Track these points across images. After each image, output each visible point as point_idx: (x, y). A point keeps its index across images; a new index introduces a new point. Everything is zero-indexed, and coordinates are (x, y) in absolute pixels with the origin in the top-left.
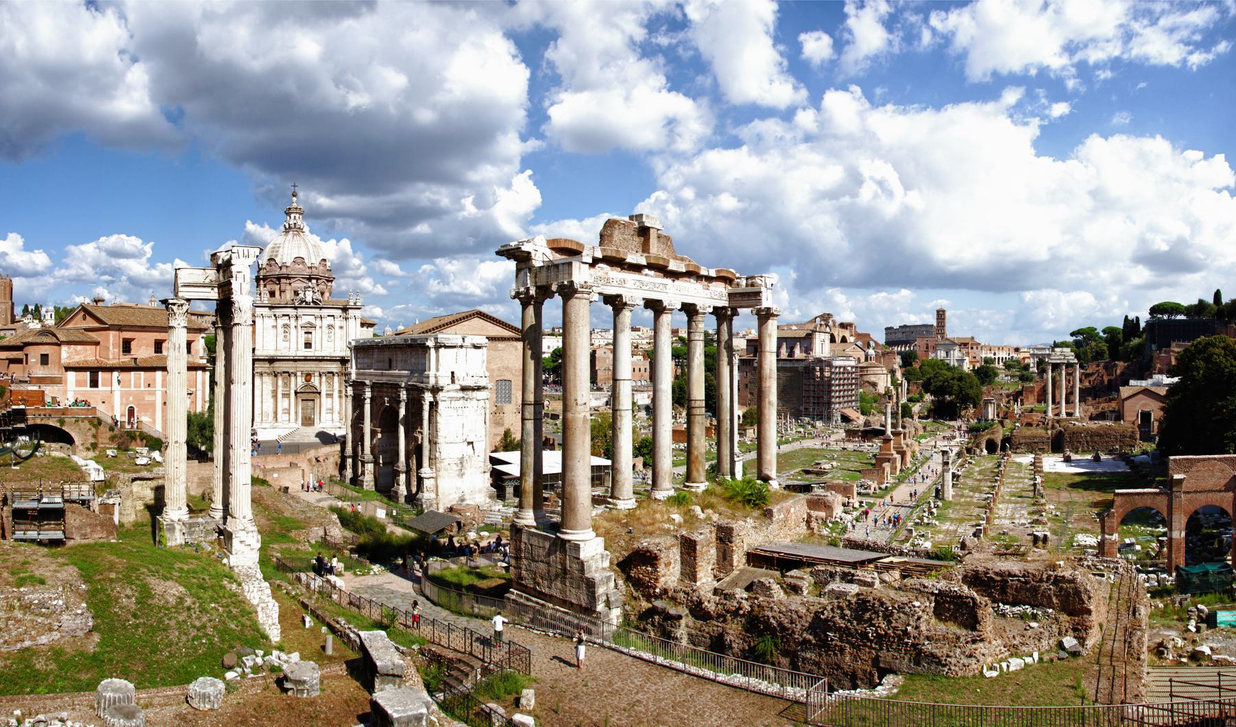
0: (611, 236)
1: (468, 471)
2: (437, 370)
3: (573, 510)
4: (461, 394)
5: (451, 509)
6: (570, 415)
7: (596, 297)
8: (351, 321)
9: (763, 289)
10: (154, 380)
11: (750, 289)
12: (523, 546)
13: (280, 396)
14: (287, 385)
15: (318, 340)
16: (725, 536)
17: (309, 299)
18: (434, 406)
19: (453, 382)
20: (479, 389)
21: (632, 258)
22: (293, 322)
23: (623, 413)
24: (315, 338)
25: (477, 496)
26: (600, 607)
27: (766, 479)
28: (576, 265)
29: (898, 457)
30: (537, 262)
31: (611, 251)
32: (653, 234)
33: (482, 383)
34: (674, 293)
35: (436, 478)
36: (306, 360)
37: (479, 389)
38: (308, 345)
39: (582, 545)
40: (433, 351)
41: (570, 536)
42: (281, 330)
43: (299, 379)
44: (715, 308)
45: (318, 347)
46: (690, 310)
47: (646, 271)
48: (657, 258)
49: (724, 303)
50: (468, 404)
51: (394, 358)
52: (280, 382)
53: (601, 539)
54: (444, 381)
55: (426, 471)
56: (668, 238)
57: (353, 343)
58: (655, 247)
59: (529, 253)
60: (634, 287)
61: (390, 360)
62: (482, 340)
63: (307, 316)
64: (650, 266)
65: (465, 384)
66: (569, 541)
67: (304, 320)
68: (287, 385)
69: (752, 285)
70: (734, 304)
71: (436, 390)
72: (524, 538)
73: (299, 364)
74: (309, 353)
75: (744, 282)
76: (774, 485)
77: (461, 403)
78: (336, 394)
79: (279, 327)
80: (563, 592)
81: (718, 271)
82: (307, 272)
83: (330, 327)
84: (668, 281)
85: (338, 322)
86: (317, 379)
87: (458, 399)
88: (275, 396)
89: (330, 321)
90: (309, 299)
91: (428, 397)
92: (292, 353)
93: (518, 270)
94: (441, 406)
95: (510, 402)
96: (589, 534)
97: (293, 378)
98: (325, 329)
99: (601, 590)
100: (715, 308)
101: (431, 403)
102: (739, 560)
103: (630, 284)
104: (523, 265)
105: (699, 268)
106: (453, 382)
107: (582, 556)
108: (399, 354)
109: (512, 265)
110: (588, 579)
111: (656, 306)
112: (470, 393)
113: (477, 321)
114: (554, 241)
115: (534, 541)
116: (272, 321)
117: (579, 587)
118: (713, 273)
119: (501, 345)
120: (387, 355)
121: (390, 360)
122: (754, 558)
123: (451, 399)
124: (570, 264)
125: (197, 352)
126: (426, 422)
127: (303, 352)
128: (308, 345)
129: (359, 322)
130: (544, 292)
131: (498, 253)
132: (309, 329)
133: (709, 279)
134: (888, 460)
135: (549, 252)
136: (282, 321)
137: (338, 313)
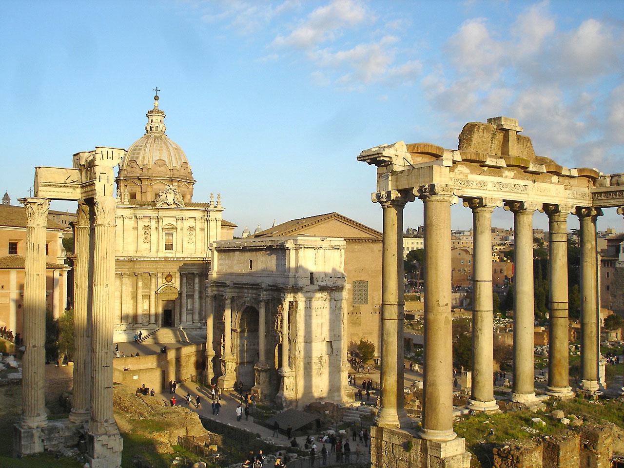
0: (470, 140)
3: (434, 410)
6: (431, 316)
7: (456, 200)
8: (212, 224)
10: (9, 281)
11: (613, 189)
12: (384, 444)
13: (140, 297)
14: (147, 286)
15: (179, 241)
17: (170, 200)
19: (312, 283)
22: (154, 222)
23: (485, 315)
24: (176, 240)
28: (436, 168)
30: (399, 166)
31: (471, 153)
32: (512, 136)
34: (536, 194)
36: (166, 260)
38: (169, 247)
39: (443, 445)
40: (293, 253)
41: (434, 435)
42: (141, 232)
43: (160, 280)
44: (579, 209)
45: (179, 248)
46: (551, 210)
47: (507, 173)
48: (518, 158)
49: (586, 203)
51: (254, 259)
52: (140, 284)
53: (462, 441)
56: (528, 140)
57: (215, 245)
58: (515, 150)
60: (494, 189)
62: (341, 242)
63: (168, 219)
65: (323, 284)
66: (431, 441)
67: (165, 222)
68: (147, 286)
69: (618, 184)
70: (598, 204)
72: (385, 437)
73: (161, 266)
74: (169, 254)
75: (608, 181)
78: (197, 296)
79: (140, 228)
81: (580, 171)
82: (170, 174)
83: (192, 229)
84: (529, 183)
85: (199, 225)
86: (178, 280)
88: (135, 297)
89: (191, 223)
90: (170, 200)
92: (153, 254)
93: (380, 175)
95: (367, 303)
96: (450, 435)
97: (153, 280)
98: (186, 232)
100: (579, 209)
101: (291, 303)
103: (490, 186)
104: (384, 170)
106: (312, 283)
111: (515, 207)
116: (130, 223)
118: (575, 173)
119: (357, 247)
120: (248, 256)
121: (251, 261)
124: (431, 168)
125: (54, 253)
126: (286, 322)
127: (164, 253)
128: (169, 247)
129: (219, 223)
130: (407, 195)
131: (361, 158)
132: (170, 231)
135: (409, 156)
136: (141, 224)
137: (198, 215)
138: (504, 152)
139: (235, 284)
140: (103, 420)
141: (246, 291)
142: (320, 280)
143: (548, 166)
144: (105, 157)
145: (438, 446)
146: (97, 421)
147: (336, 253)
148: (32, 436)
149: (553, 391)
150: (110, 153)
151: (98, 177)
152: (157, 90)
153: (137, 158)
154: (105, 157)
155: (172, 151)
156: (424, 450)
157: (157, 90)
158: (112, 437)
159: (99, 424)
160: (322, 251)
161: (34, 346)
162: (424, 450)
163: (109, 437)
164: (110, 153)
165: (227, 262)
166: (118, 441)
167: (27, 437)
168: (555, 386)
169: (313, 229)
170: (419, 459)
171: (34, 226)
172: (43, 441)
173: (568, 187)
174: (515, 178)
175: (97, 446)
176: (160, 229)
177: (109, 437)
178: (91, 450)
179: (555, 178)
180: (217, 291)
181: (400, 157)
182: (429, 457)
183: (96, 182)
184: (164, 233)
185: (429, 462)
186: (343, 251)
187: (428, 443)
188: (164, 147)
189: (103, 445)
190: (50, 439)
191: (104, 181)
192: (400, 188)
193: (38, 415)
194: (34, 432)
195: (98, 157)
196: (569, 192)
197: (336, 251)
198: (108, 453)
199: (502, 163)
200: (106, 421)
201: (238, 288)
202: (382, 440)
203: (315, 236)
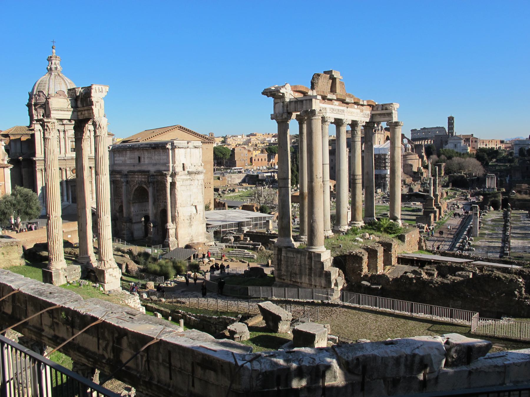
1: (195, 223)
2: (174, 162)
4: (188, 177)
5: (188, 247)
9: (393, 111)
16: (387, 247)
18: (173, 184)
20: (198, 173)
21: (329, 96)
22: (62, 134)
25: (200, 237)
26: (333, 286)
27: (395, 219)
29: (437, 210)
32: (338, 81)
33: (201, 169)
35: (176, 229)
37: (198, 173)
43: (68, 172)
50: (192, 183)
51: (142, 156)
54: (179, 169)
55: (170, 225)
59: (283, 94)
61: (139, 158)
64: (338, 100)
65: (190, 170)
66: (314, 252)
71: (174, 175)
72: (283, 254)
76: (400, 222)
77: (189, 182)
80: (310, 280)
81: (368, 102)
84: (344, 108)
87: (187, 180)
91: (169, 180)
93: (275, 104)
94: (178, 185)
97: (64, 173)
99: (333, 277)
102: (394, 261)
104: (279, 101)
105: (359, 100)
106: (184, 169)
107: (322, 260)
108: (146, 154)
109: (271, 99)
110: (326, 272)
112: (193, 176)
113: (177, 133)
114: (295, 87)
115: (291, 255)
117: (320, 276)
118: (365, 103)
120: (137, 154)
121: (139, 158)
122: (402, 260)
123: (183, 180)
131: (263, 93)
133: (362, 105)
134: (431, 212)
135: (292, 92)
138: (333, 89)
139: (128, 172)
140: (108, 260)
141: (136, 176)
142: (188, 168)
143: (354, 99)
144: (98, 91)
145: (319, 255)
146: (104, 261)
147: (197, 150)
148: (59, 274)
149: (355, 224)
150: (100, 88)
151: (94, 104)
152: (53, 42)
153: (44, 89)
154: (98, 91)
155: (68, 84)
156: (310, 258)
157: (53, 42)
158: (115, 269)
159: (106, 262)
160: (188, 149)
161: (55, 217)
162: (310, 258)
163: (113, 269)
164: (100, 88)
165: (121, 158)
166: (118, 271)
167: (56, 275)
168: (357, 221)
169: (164, 136)
170: (307, 263)
171: (50, 137)
172: (66, 277)
173: (362, 111)
174: (339, 105)
175: (107, 276)
176: (67, 138)
177: (113, 269)
178: (102, 279)
179: (356, 106)
180: (116, 177)
181: (289, 94)
182: (313, 262)
183: (93, 107)
184: (69, 141)
185: (313, 264)
186: (201, 149)
187: (312, 254)
188: (63, 81)
189: (110, 275)
190: (70, 275)
191: (98, 107)
192: (289, 111)
193: (61, 261)
194: (60, 271)
195: (93, 91)
196: (362, 113)
197: (197, 149)
198: (113, 279)
199: (334, 97)
200: (110, 260)
201: (130, 175)
202: (281, 255)
203: (183, 140)
